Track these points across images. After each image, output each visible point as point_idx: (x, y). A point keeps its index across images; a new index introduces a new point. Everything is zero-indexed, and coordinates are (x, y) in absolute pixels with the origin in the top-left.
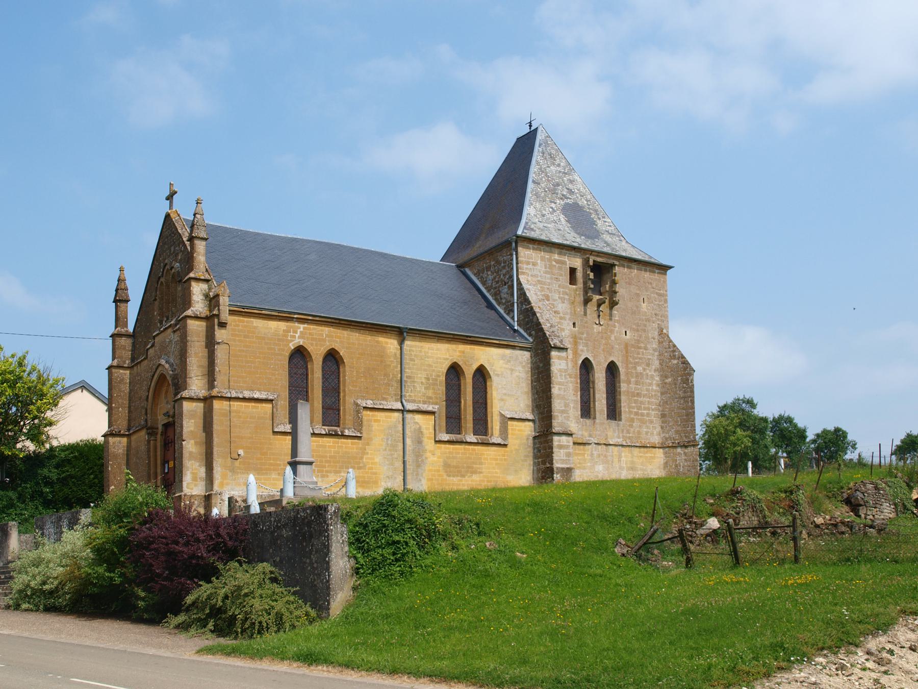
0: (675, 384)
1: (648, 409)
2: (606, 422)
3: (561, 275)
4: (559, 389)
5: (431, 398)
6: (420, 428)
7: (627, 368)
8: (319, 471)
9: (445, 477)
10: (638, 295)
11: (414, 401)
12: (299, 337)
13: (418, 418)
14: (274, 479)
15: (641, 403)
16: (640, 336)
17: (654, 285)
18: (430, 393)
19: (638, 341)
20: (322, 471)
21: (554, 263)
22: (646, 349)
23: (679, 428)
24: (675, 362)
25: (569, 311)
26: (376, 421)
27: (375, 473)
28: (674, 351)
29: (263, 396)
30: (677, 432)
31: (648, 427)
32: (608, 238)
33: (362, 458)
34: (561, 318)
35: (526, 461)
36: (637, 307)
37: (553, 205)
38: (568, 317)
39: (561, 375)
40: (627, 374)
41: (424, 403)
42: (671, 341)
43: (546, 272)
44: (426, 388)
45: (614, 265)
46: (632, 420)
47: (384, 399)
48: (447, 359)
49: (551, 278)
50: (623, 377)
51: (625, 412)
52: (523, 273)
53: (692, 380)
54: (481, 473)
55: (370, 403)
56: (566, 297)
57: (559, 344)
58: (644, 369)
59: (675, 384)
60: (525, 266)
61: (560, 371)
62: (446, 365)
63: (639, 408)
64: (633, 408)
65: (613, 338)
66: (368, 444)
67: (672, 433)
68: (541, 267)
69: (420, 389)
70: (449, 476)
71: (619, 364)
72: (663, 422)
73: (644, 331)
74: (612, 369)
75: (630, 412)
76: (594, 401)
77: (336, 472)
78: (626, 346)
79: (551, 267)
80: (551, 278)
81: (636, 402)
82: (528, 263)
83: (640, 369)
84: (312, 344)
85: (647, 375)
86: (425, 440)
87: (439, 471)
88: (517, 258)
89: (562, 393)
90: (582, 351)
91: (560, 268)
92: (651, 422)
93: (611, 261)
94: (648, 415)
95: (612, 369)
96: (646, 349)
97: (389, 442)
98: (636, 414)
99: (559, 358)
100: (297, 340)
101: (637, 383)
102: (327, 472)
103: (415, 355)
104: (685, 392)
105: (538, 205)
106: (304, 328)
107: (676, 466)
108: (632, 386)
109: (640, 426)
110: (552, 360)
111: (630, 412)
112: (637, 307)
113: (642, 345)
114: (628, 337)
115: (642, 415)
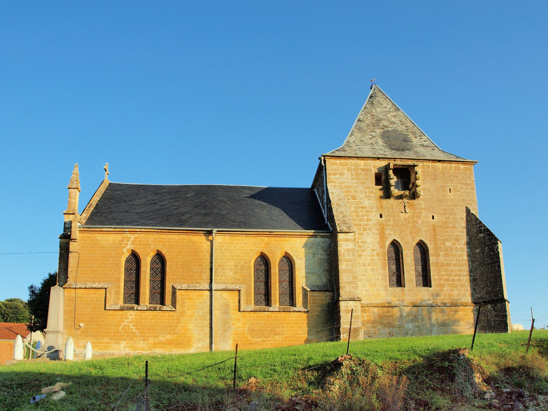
0: (483, 253)
1: (460, 275)
2: (415, 288)
3: (367, 179)
4: (347, 265)
5: (238, 280)
6: (227, 302)
7: (435, 243)
8: (141, 337)
9: (250, 338)
10: (444, 186)
11: (222, 283)
12: (131, 244)
13: (226, 294)
14: (106, 343)
15: (452, 271)
16: (448, 218)
17: (460, 178)
18: (238, 276)
19: (446, 222)
20: (144, 336)
21: (360, 171)
22: (454, 227)
23: (489, 289)
24: (482, 235)
25: (375, 206)
26: (189, 299)
27: (188, 337)
28: (480, 227)
29: (100, 286)
30: (488, 292)
31: (459, 290)
32: (421, 150)
33: (177, 326)
34: (368, 211)
35: (328, 323)
36: (444, 196)
37: (373, 134)
38: (374, 210)
39: (349, 254)
40: (436, 249)
41: (233, 283)
42: (477, 219)
43: (353, 179)
44: (234, 273)
45: (414, 166)
46: (443, 286)
47: (197, 283)
48: (253, 250)
49: (358, 183)
50: (431, 252)
51: (435, 279)
52: (332, 182)
53: (497, 248)
54: (282, 334)
55: (185, 286)
56: (373, 195)
57: (345, 229)
58: (453, 244)
59: (483, 253)
60: (332, 177)
61: (348, 250)
62: (254, 256)
63: (450, 275)
64: (444, 275)
65: (420, 222)
66: (182, 316)
67: (483, 293)
68: (347, 175)
69: (230, 274)
70: (254, 337)
71: (427, 242)
72: (475, 285)
73: (452, 214)
74: (422, 247)
75: (440, 279)
76: (404, 273)
77: (155, 337)
78: (434, 228)
79: (357, 174)
80: (358, 183)
81: (445, 270)
82: (335, 174)
83: (448, 244)
84: (140, 249)
85: (457, 248)
86: (231, 311)
87: (244, 334)
88: (326, 172)
89: (350, 267)
90: (390, 234)
91: (365, 175)
92: (463, 286)
93: (410, 163)
94: (459, 280)
95: (422, 247)
96: (454, 227)
97: (200, 314)
98: (446, 280)
99: (347, 240)
100: (129, 246)
101: (446, 255)
102: (147, 337)
103: (225, 250)
104: (491, 259)
105: (359, 135)
106: (135, 238)
107: (488, 320)
108: (442, 258)
109: (451, 290)
110: (339, 243)
111: (440, 279)
112: (444, 196)
113: (450, 225)
114: (435, 220)
115: (453, 280)
